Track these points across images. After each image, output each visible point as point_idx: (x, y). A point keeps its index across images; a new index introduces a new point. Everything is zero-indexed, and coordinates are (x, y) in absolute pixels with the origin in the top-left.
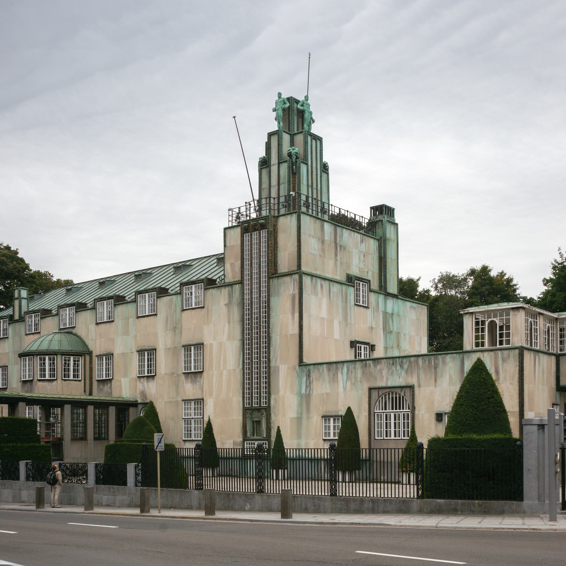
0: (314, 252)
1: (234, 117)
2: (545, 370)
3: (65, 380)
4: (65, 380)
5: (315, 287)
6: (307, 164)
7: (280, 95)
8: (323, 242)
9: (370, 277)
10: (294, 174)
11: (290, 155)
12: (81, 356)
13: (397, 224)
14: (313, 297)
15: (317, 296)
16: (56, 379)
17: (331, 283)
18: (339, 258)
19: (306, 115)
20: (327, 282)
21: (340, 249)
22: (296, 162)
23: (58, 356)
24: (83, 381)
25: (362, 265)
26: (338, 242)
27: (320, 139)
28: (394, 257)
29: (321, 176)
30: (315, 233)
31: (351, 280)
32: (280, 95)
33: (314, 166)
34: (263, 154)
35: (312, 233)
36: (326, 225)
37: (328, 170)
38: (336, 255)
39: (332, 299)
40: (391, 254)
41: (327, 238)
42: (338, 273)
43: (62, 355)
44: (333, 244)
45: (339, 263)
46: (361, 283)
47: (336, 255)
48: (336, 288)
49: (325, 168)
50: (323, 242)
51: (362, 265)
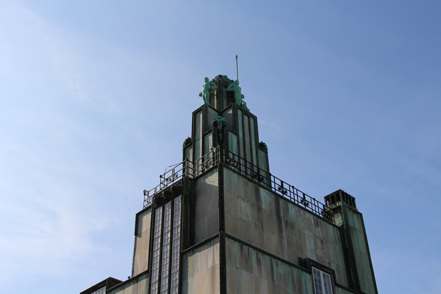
0: (245, 218)
5: (247, 259)
6: (237, 135)
7: (207, 79)
8: (259, 209)
9: (333, 267)
11: (215, 124)
14: (244, 273)
15: (251, 272)
17: (274, 261)
18: (285, 236)
19: (237, 96)
20: (267, 258)
21: (287, 226)
25: (320, 253)
27: (255, 118)
28: (364, 251)
31: (305, 265)
32: (207, 79)
33: (247, 140)
34: (189, 135)
35: (243, 195)
38: (280, 231)
39: (277, 283)
40: (357, 244)
41: (264, 206)
42: (286, 253)
44: (275, 217)
45: (286, 242)
46: (321, 272)
47: (280, 231)
48: (282, 269)
49: (262, 147)
51: (320, 253)
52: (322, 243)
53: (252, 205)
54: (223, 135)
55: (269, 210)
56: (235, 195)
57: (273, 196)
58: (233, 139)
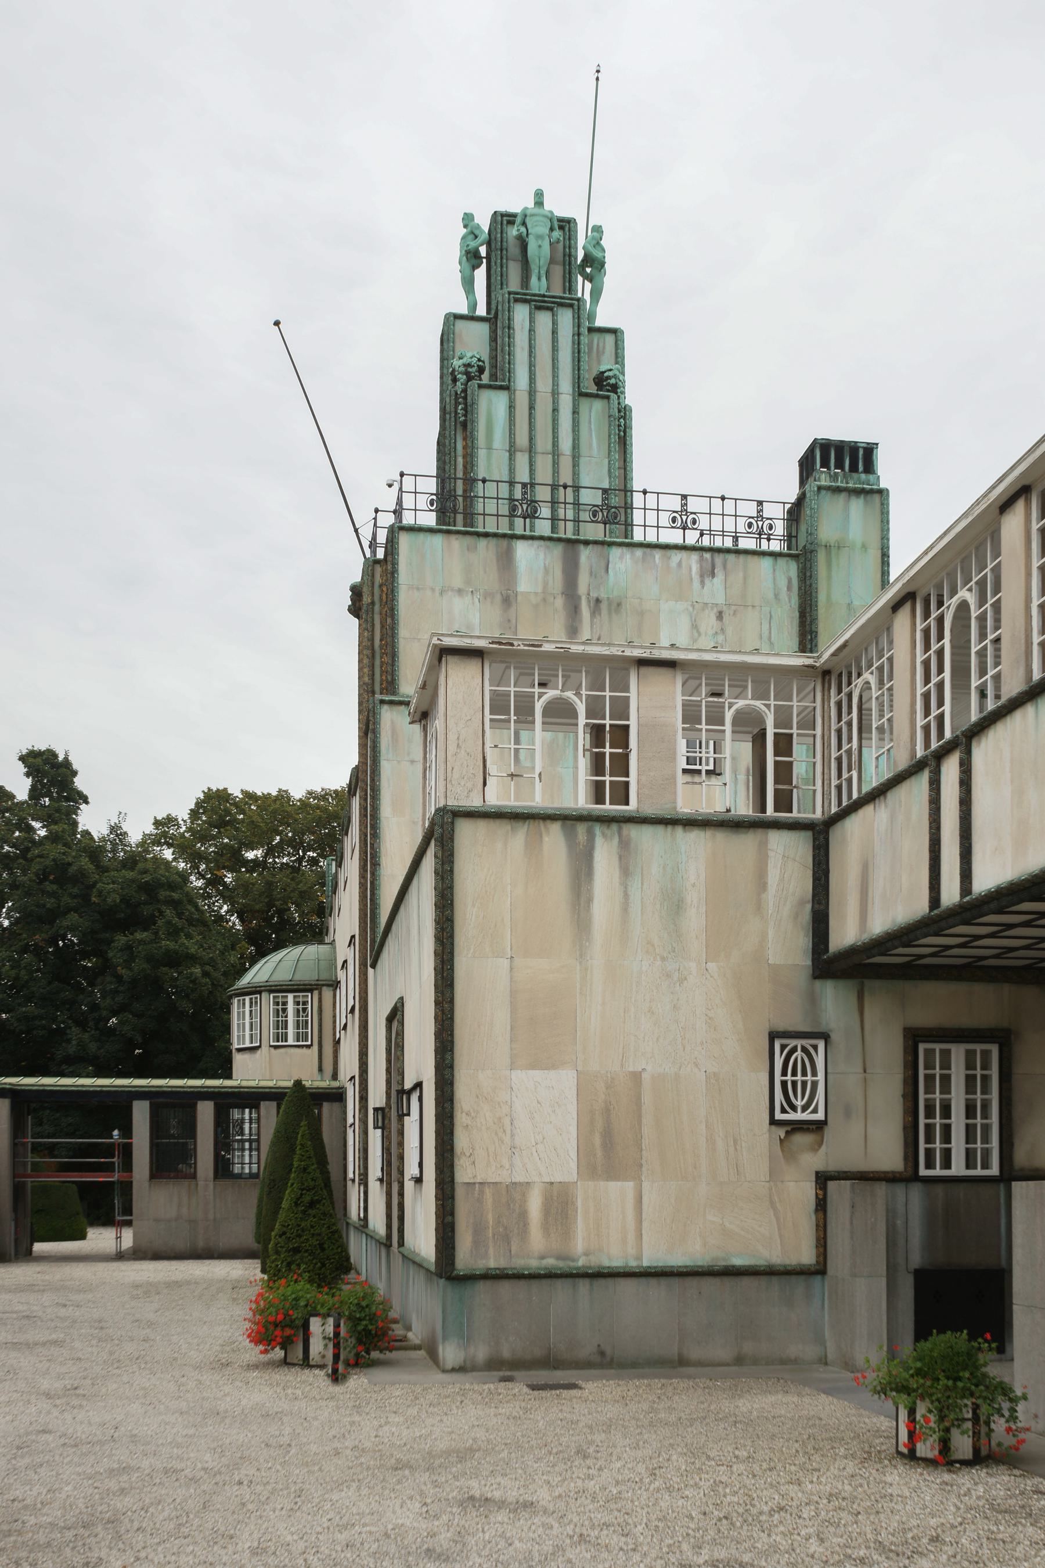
1: (277, 323)
2: (694, 897)
3: (276, 1047)
4: (276, 1047)
8: (507, 601)
10: (464, 425)
12: (311, 991)
13: (882, 493)
16: (260, 1047)
22: (465, 391)
23: (263, 994)
24: (316, 1047)
26: (582, 589)
29: (575, 412)
30: (468, 582)
33: (544, 386)
35: (458, 582)
36: (523, 551)
37: (615, 388)
41: (524, 585)
43: (271, 991)
44: (559, 602)
50: (507, 601)
52: (720, 616)
53: (487, 595)
54: (465, 409)
55: (540, 590)
56: (433, 590)
57: (558, 550)
58: (492, 407)
